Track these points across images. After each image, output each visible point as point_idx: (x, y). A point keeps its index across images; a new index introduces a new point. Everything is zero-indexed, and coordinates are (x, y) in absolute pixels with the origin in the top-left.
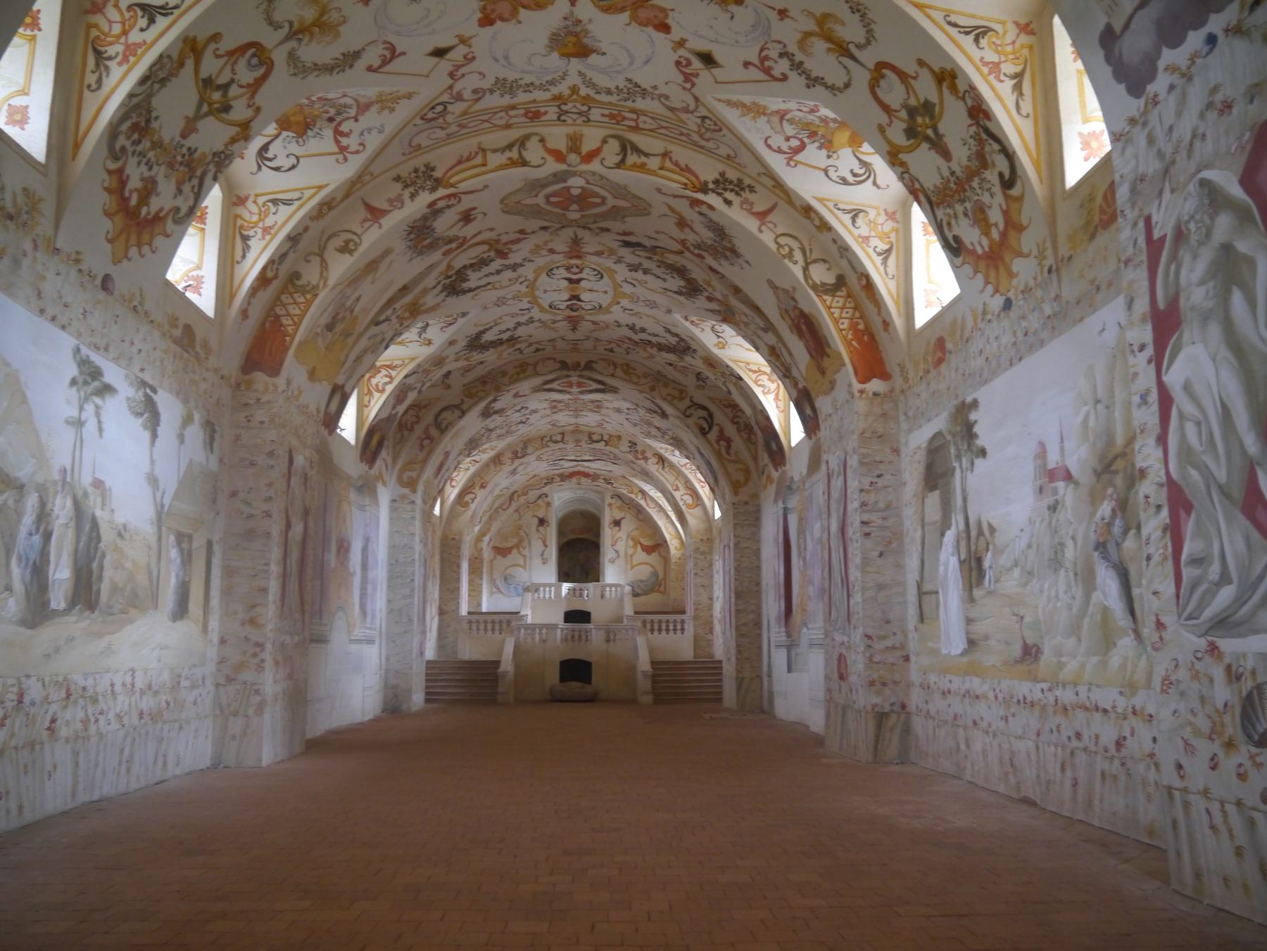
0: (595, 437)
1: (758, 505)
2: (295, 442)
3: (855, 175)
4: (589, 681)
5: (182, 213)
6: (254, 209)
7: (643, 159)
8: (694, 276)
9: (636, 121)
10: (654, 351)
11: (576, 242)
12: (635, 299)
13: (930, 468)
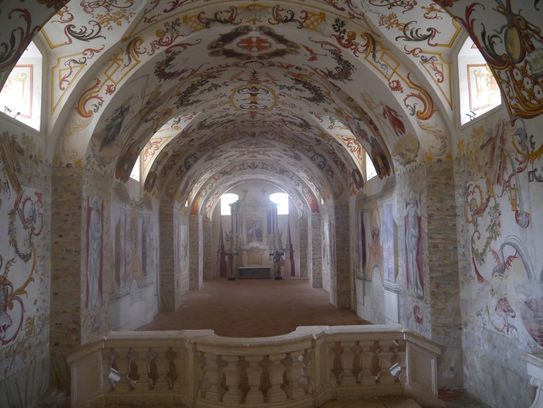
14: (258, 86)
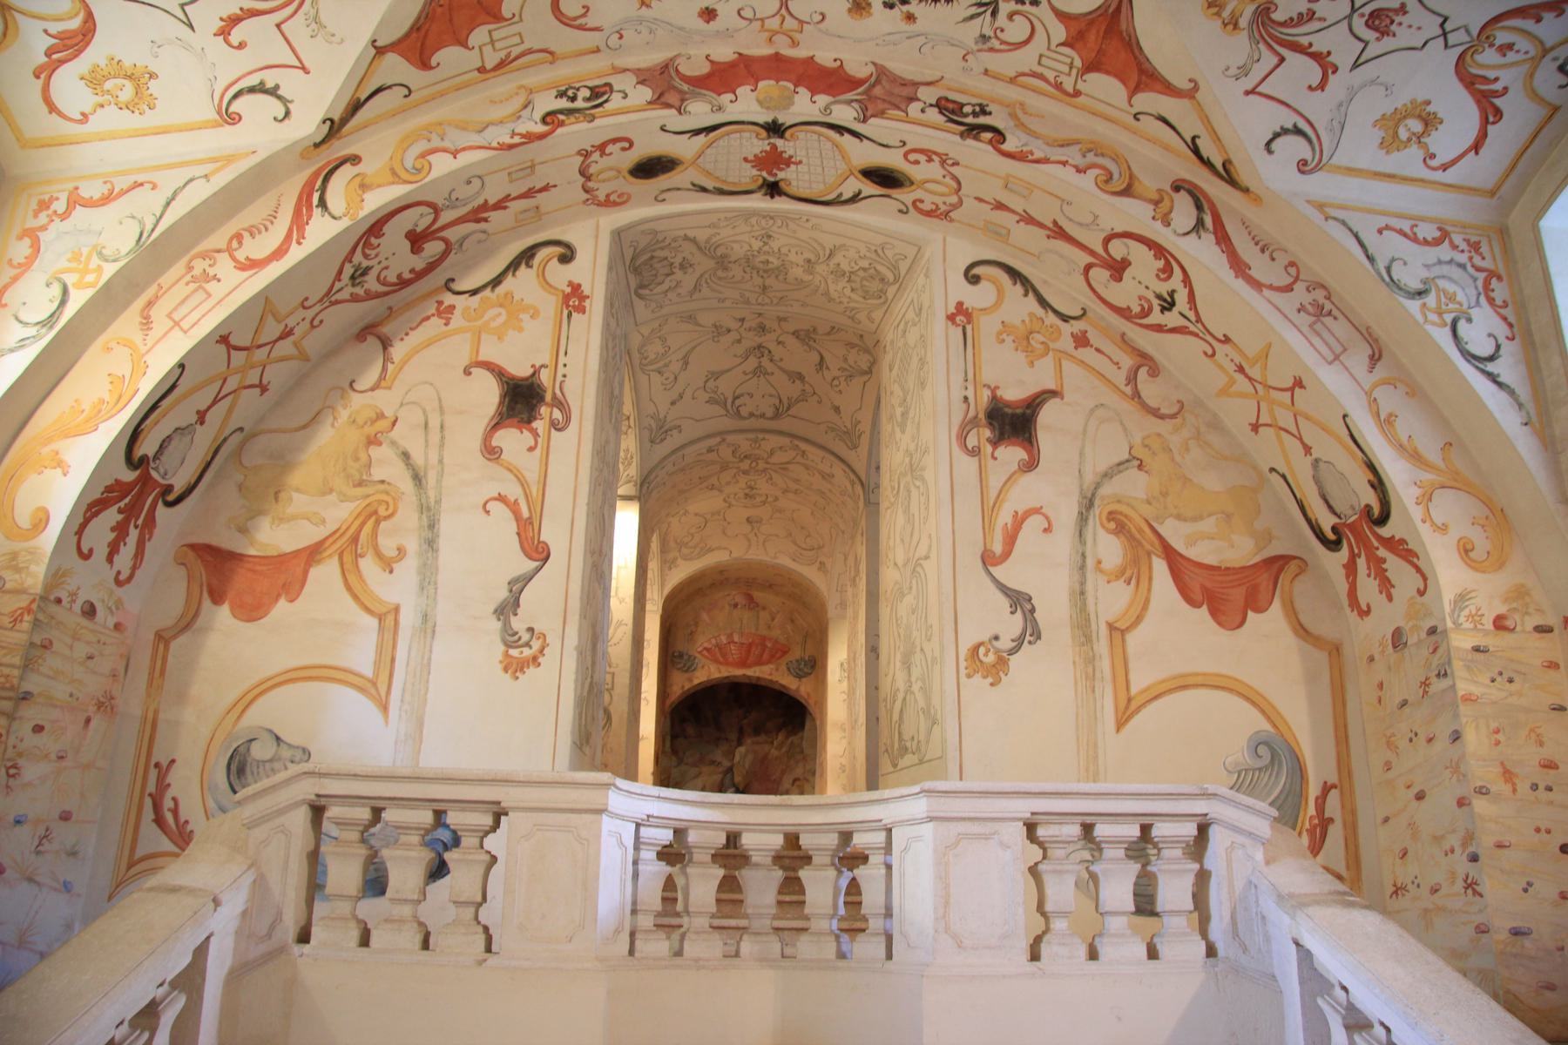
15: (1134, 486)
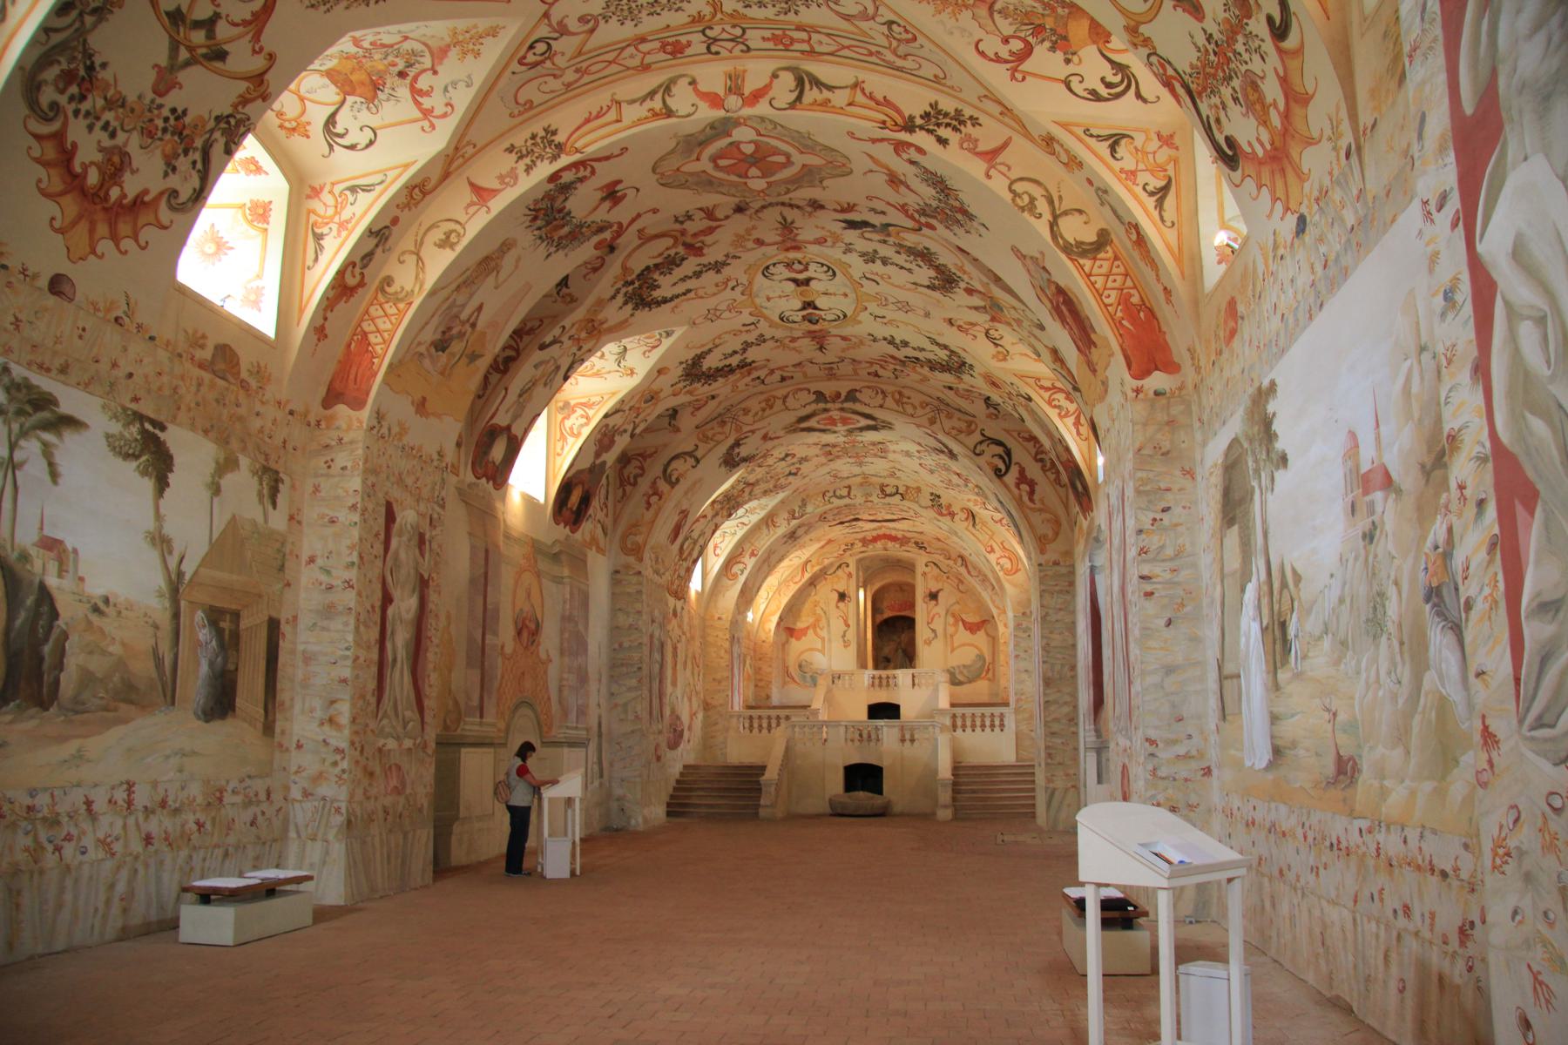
0: (888, 490)
1: (1073, 566)
2: (396, 493)
3: (1109, 85)
4: (881, 793)
5: (183, 197)
6: (329, 200)
7: (826, 94)
8: (942, 261)
9: (809, 41)
10: (926, 371)
11: (787, 227)
12: (884, 303)
13: (1227, 492)
14: (807, 326)
15: (957, 607)
